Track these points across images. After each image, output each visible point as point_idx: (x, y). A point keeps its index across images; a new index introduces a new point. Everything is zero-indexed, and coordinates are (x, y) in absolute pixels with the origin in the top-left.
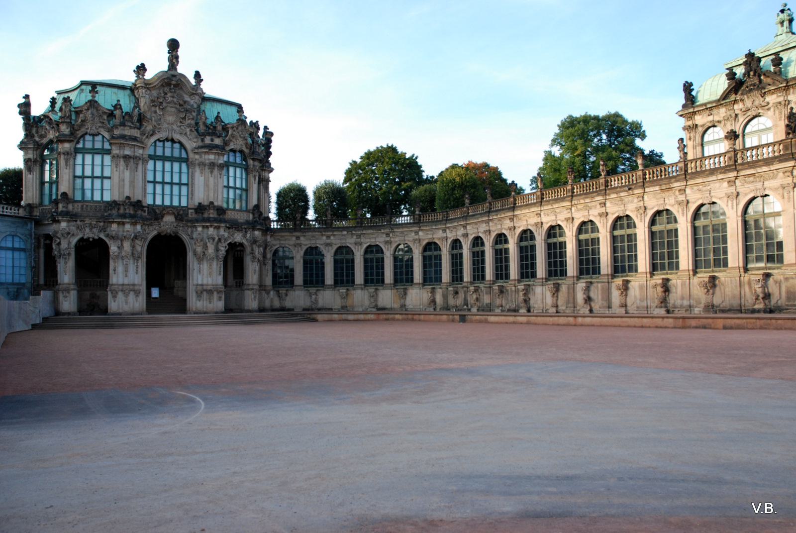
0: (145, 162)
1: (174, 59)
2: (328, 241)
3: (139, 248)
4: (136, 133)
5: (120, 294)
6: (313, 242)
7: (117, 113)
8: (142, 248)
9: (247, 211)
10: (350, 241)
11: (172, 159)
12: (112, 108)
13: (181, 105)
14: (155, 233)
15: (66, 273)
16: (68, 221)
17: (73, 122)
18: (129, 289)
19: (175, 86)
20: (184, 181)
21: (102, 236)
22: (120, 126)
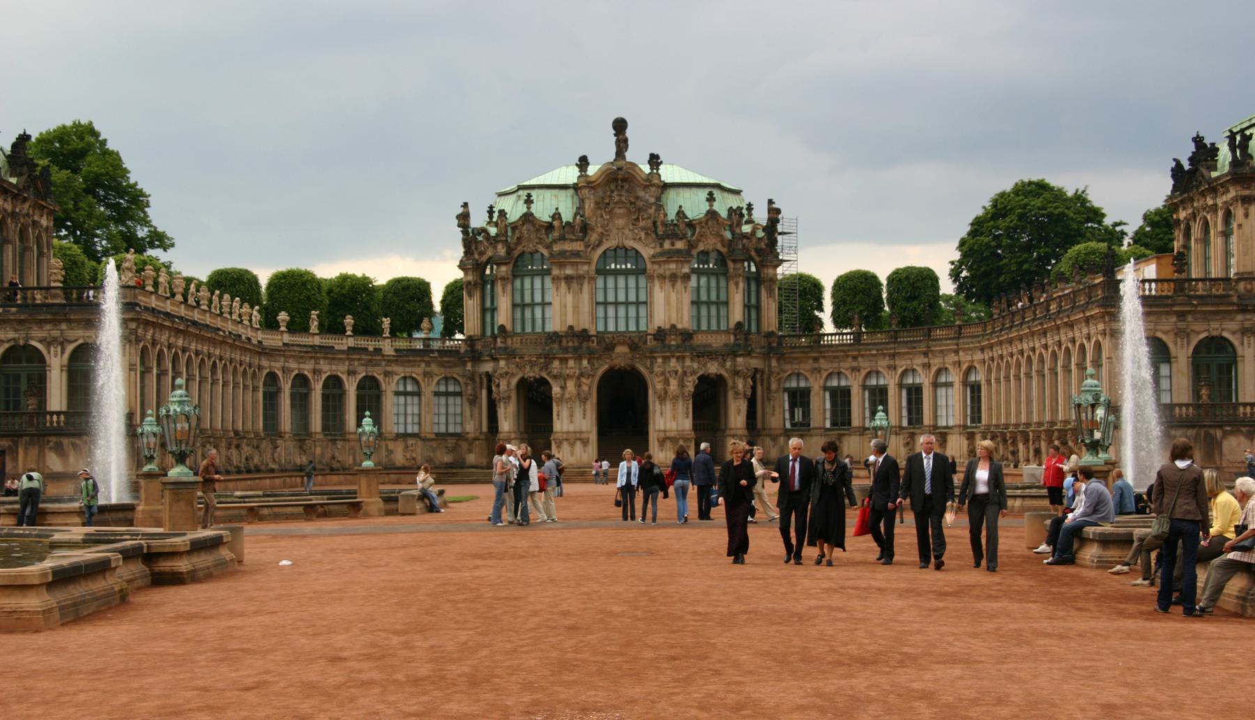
0: (592, 280)
1: (622, 145)
2: (855, 364)
3: (585, 388)
5: (565, 445)
6: (836, 365)
7: (556, 223)
8: (590, 386)
11: (626, 273)
12: (550, 220)
13: (631, 203)
14: (606, 367)
16: (507, 359)
17: (509, 240)
18: (577, 438)
19: (624, 180)
21: (544, 375)
22: (560, 240)
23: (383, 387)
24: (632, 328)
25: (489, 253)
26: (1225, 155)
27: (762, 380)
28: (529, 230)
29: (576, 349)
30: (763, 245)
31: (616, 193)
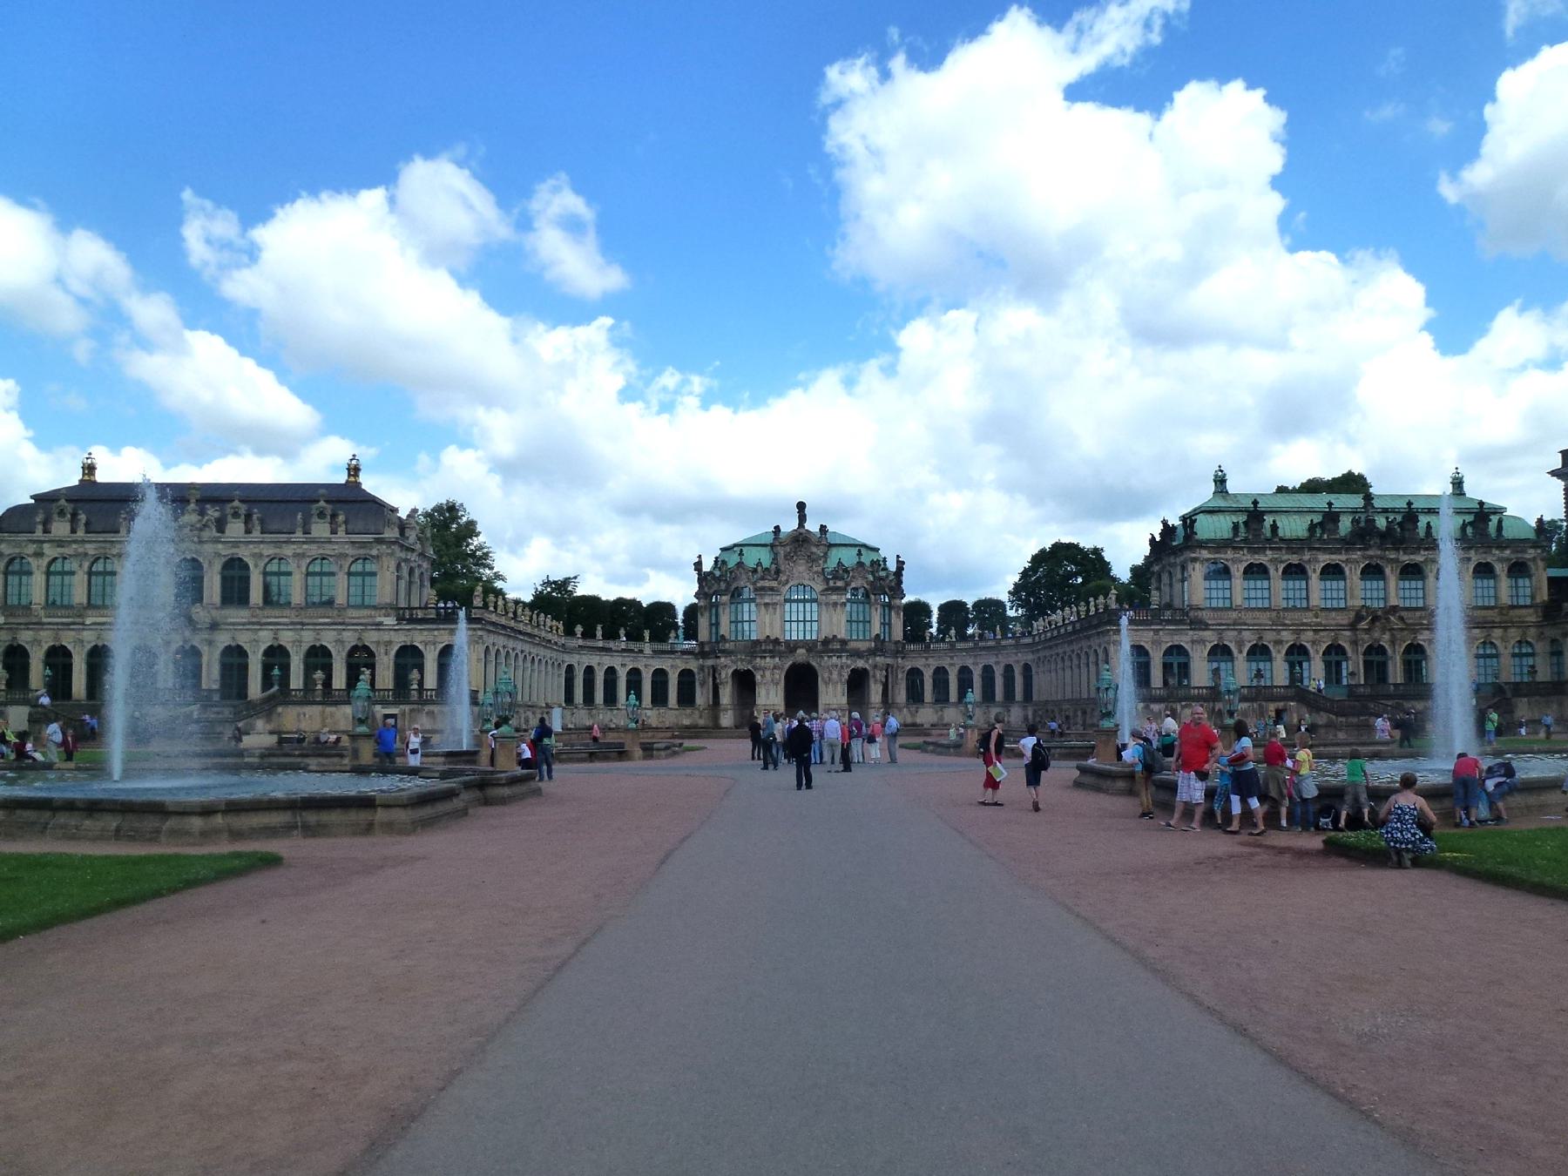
1: (802, 519)
2: (952, 662)
4: (774, 584)
7: (759, 568)
8: (780, 676)
9: (870, 640)
10: (969, 662)
11: (804, 601)
13: (808, 556)
15: (726, 695)
20: (815, 618)
21: (750, 668)
23: (644, 674)
24: (808, 638)
25: (715, 587)
26: (1181, 533)
27: (892, 672)
28: (740, 573)
29: (770, 651)
30: (893, 584)
31: (798, 550)
